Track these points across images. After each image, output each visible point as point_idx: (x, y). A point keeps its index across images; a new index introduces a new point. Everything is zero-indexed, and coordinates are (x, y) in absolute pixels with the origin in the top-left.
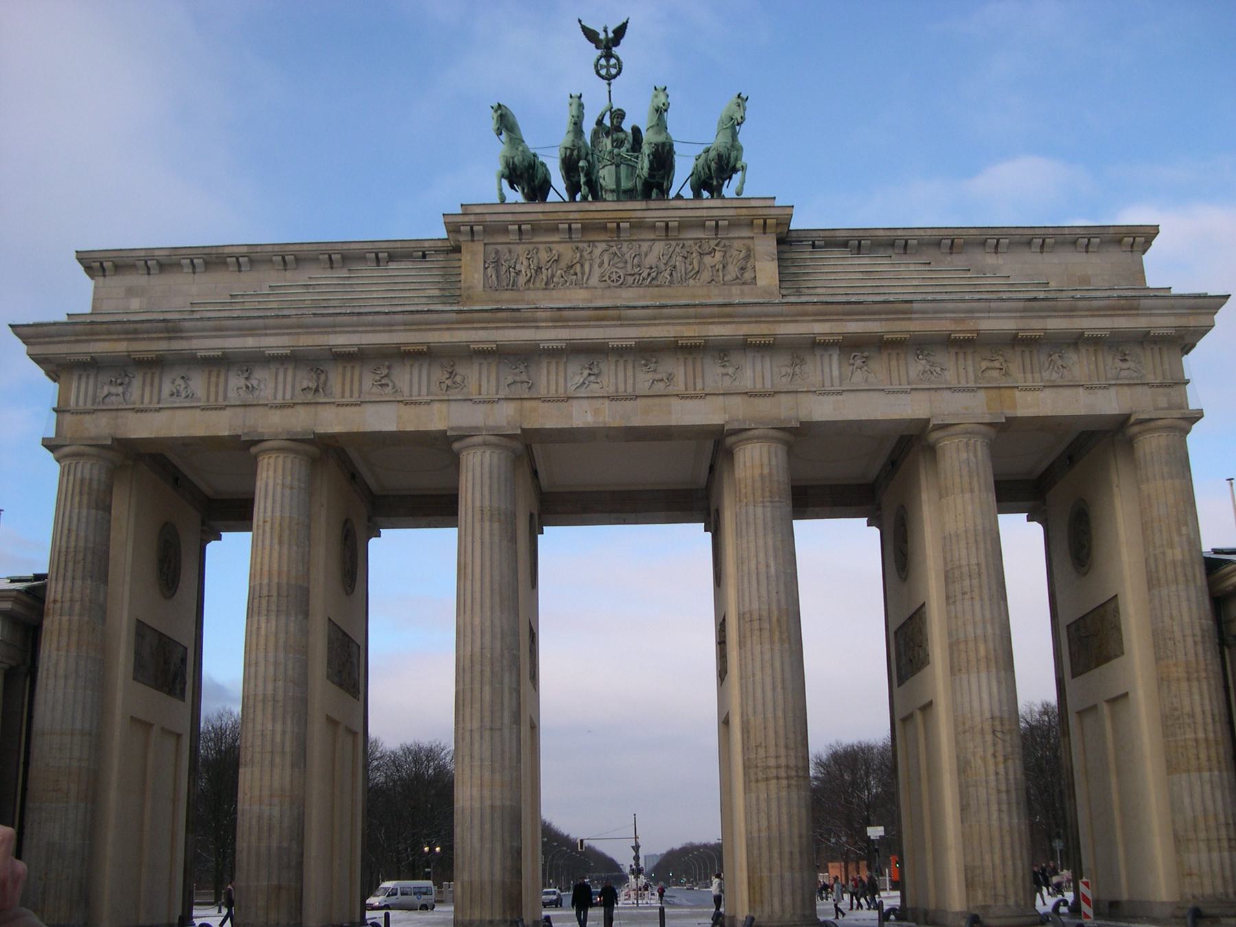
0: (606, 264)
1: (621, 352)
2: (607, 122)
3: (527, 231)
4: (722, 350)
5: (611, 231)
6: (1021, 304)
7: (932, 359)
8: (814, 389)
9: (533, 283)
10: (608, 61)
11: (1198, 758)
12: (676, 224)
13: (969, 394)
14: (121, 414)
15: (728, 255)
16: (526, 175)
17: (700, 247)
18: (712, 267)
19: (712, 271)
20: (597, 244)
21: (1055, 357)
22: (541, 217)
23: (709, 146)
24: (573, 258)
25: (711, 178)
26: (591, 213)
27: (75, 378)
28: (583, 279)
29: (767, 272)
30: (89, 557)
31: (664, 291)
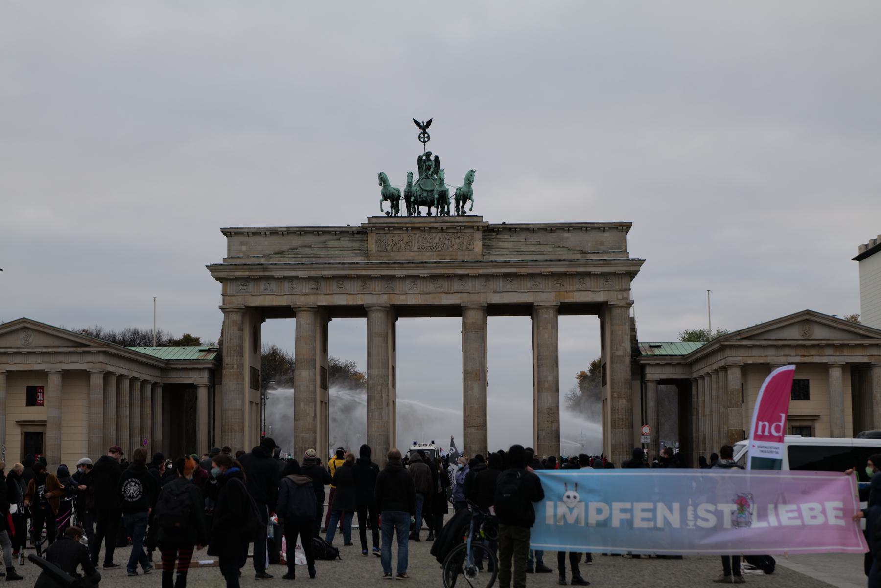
1: (425, 277)
2: (424, 158)
4: (461, 277)
6: (567, 263)
7: (535, 280)
8: (492, 291)
10: (424, 135)
11: (619, 424)
12: (445, 228)
13: (549, 294)
14: (246, 296)
20: (418, 234)
21: (581, 280)
22: (396, 225)
27: (228, 283)
29: (478, 246)
30: (238, 348)
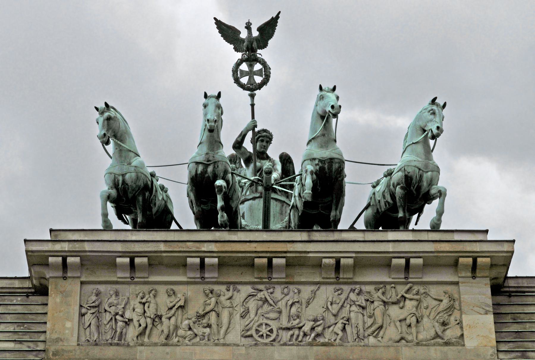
0: (252, 314)
3: (142, 266)
5: (260, 269)
9: (149, 337)
10: (251, 66)
12: (351, 261)
15: (425, 304)
16: (140, 198)
17: (383, 293)
18: (400, 321)
19: (401, 326)
20: (239, 287)
23: (392, 167)
24: (206, 304)
25: (393, 208)
26: (233, 244)
28: (219, 332)
31: (331, 348)
